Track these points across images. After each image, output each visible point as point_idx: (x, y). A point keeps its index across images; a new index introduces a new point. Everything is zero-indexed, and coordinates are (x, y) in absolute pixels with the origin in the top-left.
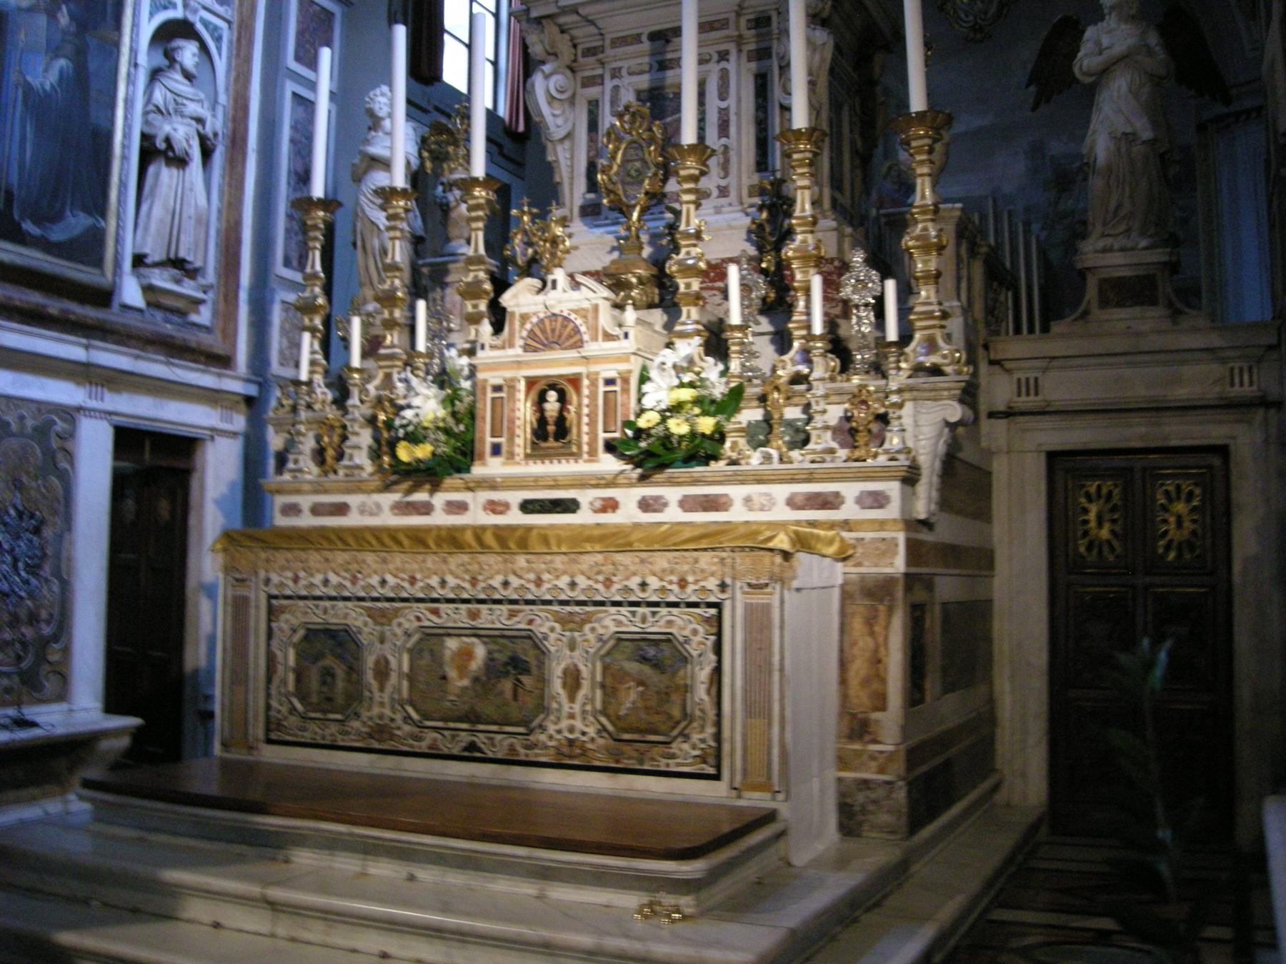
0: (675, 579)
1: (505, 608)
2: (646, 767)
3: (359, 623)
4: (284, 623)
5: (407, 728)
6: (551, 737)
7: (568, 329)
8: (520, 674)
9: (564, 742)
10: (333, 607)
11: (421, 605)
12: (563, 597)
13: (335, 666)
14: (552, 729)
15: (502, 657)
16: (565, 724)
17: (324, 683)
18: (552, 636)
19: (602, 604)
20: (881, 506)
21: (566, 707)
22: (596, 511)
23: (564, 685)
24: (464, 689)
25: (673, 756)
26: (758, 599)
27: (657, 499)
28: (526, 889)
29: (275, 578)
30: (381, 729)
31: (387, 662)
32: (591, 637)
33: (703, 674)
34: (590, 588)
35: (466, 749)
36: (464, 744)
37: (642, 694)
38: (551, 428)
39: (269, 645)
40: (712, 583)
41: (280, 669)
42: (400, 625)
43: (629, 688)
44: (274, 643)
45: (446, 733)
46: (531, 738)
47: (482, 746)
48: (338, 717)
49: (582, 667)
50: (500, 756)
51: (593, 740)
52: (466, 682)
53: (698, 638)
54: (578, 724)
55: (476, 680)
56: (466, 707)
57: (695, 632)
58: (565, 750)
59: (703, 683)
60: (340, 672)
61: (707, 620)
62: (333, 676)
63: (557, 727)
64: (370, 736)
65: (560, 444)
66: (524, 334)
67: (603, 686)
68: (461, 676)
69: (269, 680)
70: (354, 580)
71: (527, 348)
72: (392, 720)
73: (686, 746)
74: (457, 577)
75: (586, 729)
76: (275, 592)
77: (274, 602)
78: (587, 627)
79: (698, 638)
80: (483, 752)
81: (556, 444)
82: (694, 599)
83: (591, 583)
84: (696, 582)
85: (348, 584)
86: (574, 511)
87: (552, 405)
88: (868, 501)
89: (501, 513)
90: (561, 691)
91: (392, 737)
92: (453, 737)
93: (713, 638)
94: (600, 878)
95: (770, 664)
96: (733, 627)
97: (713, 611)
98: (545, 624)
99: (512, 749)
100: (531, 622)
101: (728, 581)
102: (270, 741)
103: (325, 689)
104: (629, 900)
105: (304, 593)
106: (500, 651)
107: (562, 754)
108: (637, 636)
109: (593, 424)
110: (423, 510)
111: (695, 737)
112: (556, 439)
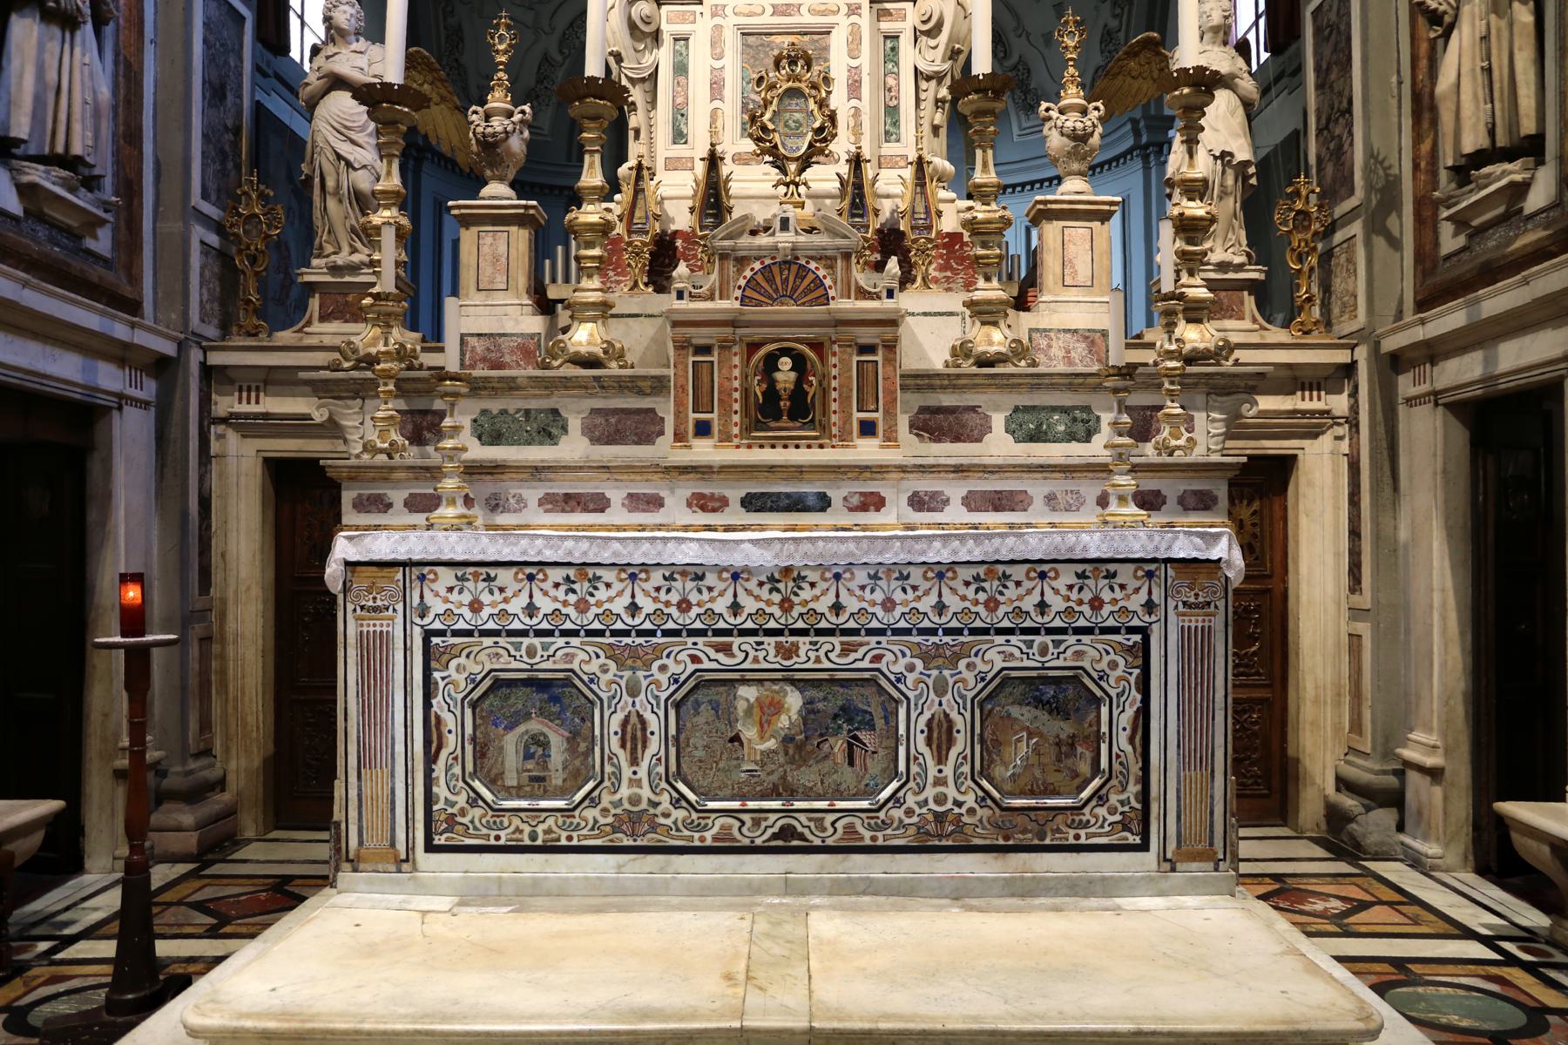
1: (836, 640)
2: (1047, 842)
3: (594, 667)
4: (456, 675)
5: (680, 814)
6: (910, 812)
7: (806, 282)
8: (857, 729)
9: (930, 817)
10: (545, 647)
11: (700, 640)
12: (926, 624)
13: (545, 730)
14: (911, 801)
15: (829, 707)
16: (930, 792)
17: (528, 756)
18: (911, 678)
19: (984, 631)
21: (932, 771)
22: (851, 510)
23: (929, 742)
24: (768, 754)
25: (1086, 825)
27: (934, 495)
29: (437, 606)
30: (633, 819)
31: (643, 722)
32: (969, 676)
33: (1125, 719)
34: (964, 610)
35: (775, 836)
36: (776, 829)
37: (1037, 751)
38: (784, 404)
39: (427, 705)
41: (451, 741)
42: (663, 668)
43: (1019, 740)
44: (436, 702)
45: (746, 817)
46: (882, 815)
47: (806, 832)
48: (560, 804)
49: (954, 715)
50: (830, 842)
51: (971, 811)
52: (771, 744)
53: (1119, 672)
54: (951, 792)
55: (787, 740)
56: (775, 778)
57: (1113, 665)
58: (931, 827)
59: (1124, 729)
60: (557, 741)
61: (1130, 650)
62: (545, 745)
63: (921, 798)
64: (615, 829)
65: (798, 424)
66: (742, 282)
67: (982, 741)
68: (762, 738)
69: (430, 759)
70: (582, 606)
71: (744, 300)
72: (656, 805)
73: (1102, 811)
74: (758, 598)
75: (961, 798)
76: (437, 625)
77: (435, 640)
78: (962, 664)
79: (1119, 672)
80: (806, 840)
81: (791, 424)
83: (762, 605)
85: (571, 611)
89: (714, 510)
90: (923, 747)
91: (654, 827)
92: (756, 823)
93: (1136, 672)
97: (1137, 638)
98: (896, 660)
99: (850, 830)
100: (877, 658)
102: (430, 848)
103: (530, 765)
106: (825, 699)
107: (928, 833)
108: (1034, 674)
109: (844, 400)
110: (591, 506)
111: (1114, 799)
112: (792, 418)
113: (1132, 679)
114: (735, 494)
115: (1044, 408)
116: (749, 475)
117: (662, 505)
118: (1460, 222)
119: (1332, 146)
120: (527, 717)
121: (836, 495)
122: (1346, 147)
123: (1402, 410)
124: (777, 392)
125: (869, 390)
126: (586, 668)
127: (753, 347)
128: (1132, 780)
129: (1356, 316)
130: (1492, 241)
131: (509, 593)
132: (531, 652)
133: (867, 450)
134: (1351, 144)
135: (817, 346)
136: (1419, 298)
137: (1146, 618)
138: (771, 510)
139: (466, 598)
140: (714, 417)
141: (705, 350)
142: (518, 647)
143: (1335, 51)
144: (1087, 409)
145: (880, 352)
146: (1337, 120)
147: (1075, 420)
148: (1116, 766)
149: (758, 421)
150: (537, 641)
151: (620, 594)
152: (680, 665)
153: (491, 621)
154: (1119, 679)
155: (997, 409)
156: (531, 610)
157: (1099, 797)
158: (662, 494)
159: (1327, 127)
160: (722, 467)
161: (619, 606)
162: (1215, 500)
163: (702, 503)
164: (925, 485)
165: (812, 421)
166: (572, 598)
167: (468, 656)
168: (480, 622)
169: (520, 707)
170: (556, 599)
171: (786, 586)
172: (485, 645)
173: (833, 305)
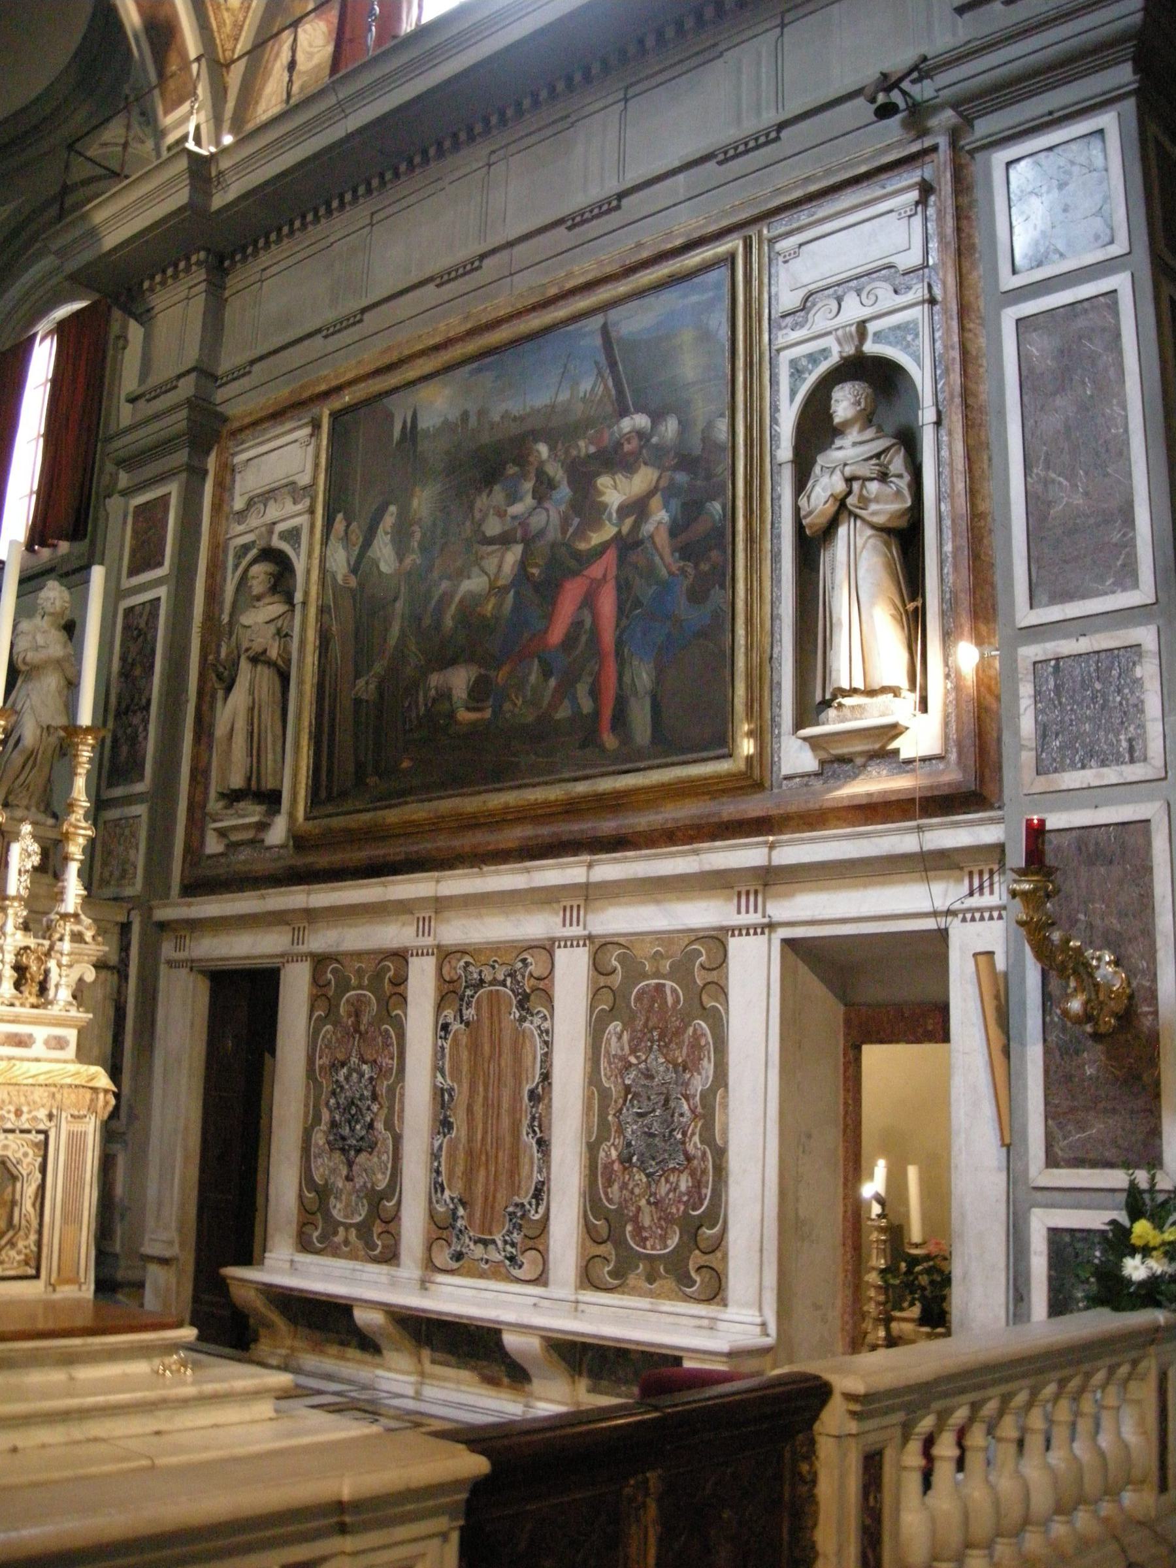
0: (12, 1109)
20: (62, 1048)
26: (78, 1127)
28: (57, 1376)
33: (31, 1190)
40: (42, 1114)
53: (29, 1159)
57: (26, 1155)
61: (36, 1145)
73: (13, 1253)
79: (29, 1159)
82: (26, 1126)
84: (30, 1112)
88: (53, 1043)
93: (40, 1159)
94: (113, 1355)
95: (82, 1179)
96: (57, 1150)
97: (41, 1137)
101: (55, 1112)
104: (140, 1368)
111: (21, 1244)
113: (37, 1165)
118: (222, 833)
119: (129, 730)
122: (140, 739)
123: (163, 969)
128: (32, 1232)
129: (134, 884)
130: (244, 855)
134: (146, 738)
136: (186, 882)
137: (48, 1124)
143: (139, 653)
146: (135, 712)
148: (24, 1222)
154: (28, 1164)
157: (12, 1244)
159: (126, 713)
162: (67, 1043)
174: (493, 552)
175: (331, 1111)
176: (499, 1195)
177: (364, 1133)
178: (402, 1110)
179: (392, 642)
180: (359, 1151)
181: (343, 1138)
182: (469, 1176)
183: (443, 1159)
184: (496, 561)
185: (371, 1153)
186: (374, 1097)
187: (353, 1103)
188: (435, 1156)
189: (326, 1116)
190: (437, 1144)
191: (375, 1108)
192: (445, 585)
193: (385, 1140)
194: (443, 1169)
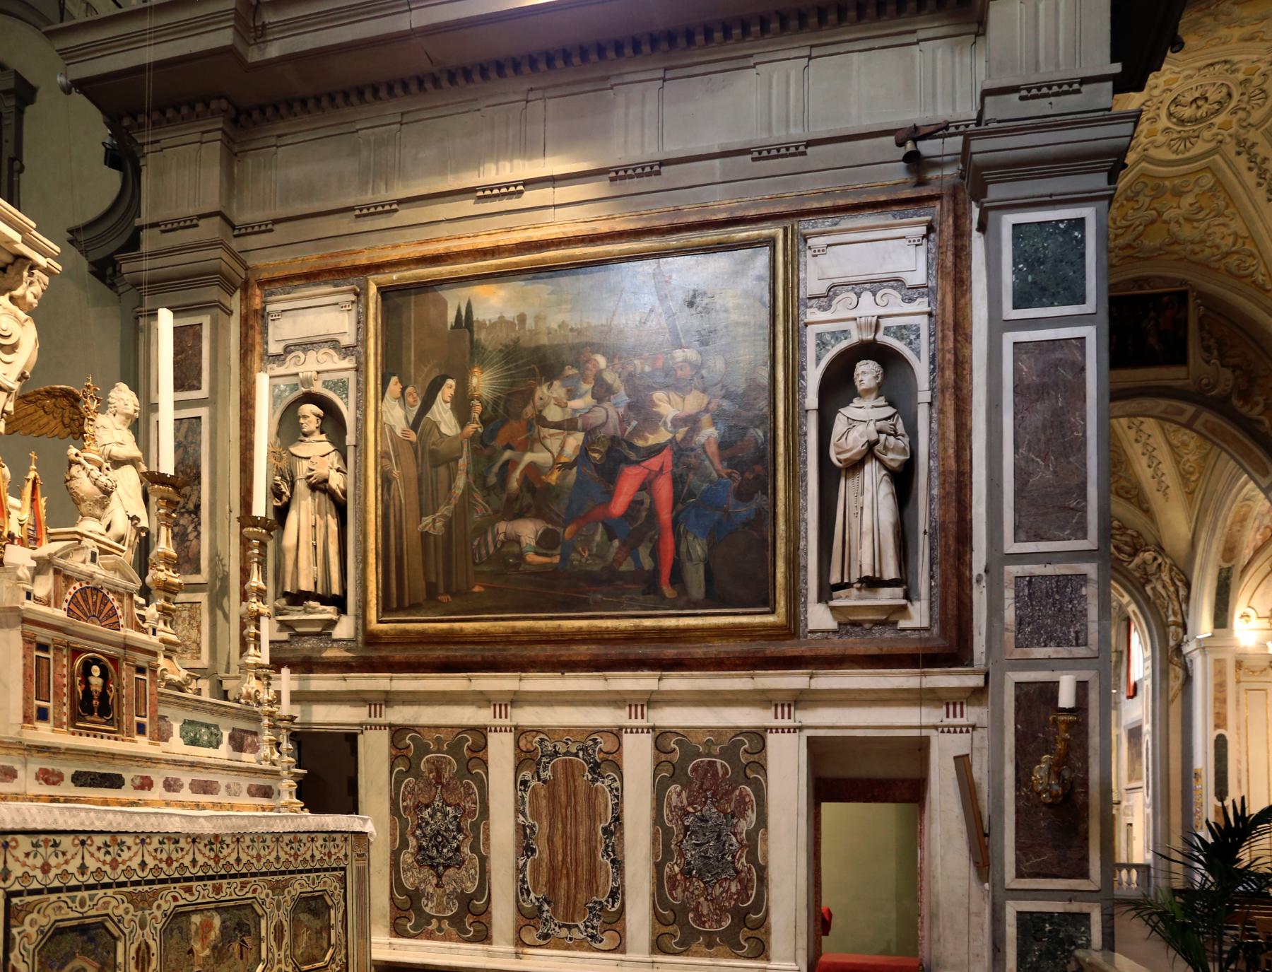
22: (136, 788)
70: (114, 864)
85: (107, 868)
86: (120, 787)
87: (96, 681)
105: (56, 884)
114: (68, 771)
115: (198, 723)
116: (78, 757)
117: (15, 776)
120: (73, 956)
121: (127, 777)
124: (91, 692)
125: (141, 700)
126: (116, 912)
127: (76, 652)
131: (69, 856)
132: (82, 904)
133: (142, 745)
135: (114, 661)
138: (90, 786)
139: (39, 862)
140: (50, 705)
141: (43, 647)
142: (73, 899)
144: (217, 727)
145: (148, 674)
147: (211, 733)
149: (80, 714)
150: (86, 894)
151: (135, 855)
152: (167, 905)
153: (56, 880)
155: (176, 720)
156: (83, 869)
158: (17, 767)
160: (68, 749)
161: (135, 864)
163: (48, 777)
164: (172, 773)
165: (112, 719)
166: (108, 858)
167: (39, 912)
168: (48, 882)
169: (68, 949)
170: (98, 860)
171: (216, 847)
172: (51, 900)
173: (122, 632)
174: (558, 434)
175: (418, 839)
176: (579, 896)
177: (451, 854)
178: (487, 838)
179: (459, 492)
180: (447, 867)
181: (432, 858)
182: (552, 884)
183: (528, 873)
184: (558, 442)
185: (459, 869)
186: (460, 830)
187: (438, 833)
188: (520, 870)
189: (413, 842)
190: (521, 863)
191: (461, 837)
192: (508, 454)
193: (471, 859)
194: (528, 878)
